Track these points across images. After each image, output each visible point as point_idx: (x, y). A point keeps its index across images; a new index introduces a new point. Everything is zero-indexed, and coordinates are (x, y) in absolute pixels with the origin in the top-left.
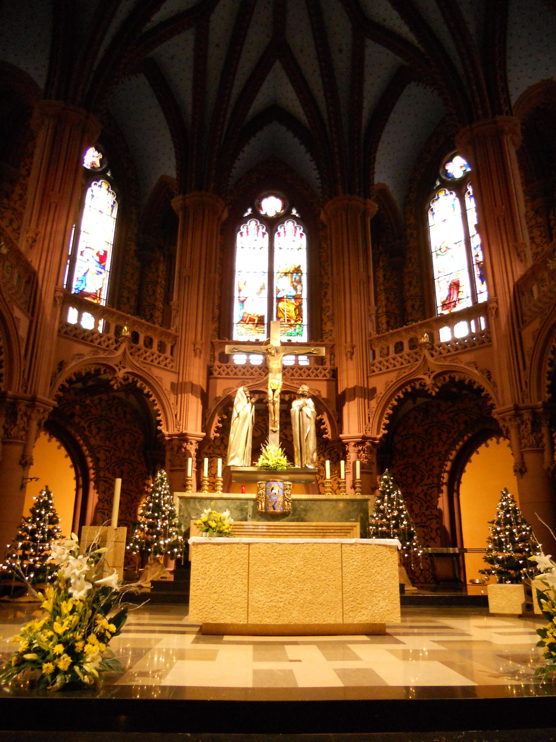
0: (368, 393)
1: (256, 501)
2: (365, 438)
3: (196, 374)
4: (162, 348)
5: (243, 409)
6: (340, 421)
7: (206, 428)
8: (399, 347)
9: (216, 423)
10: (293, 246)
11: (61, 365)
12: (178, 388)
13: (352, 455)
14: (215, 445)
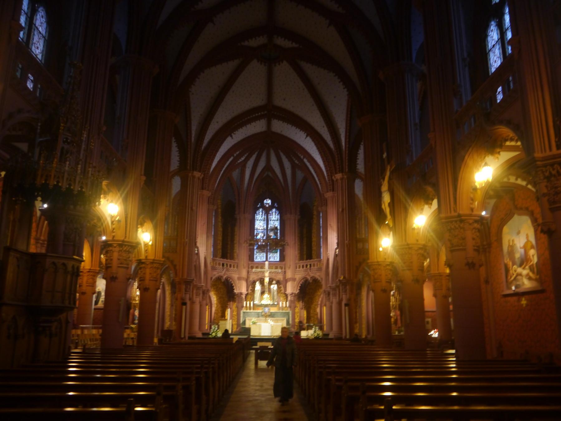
1: (262, 312)
2: (292, 293)
3: (244, 273)
4: (234, 267)
7: (247, 290)
8: (303, 267)
9: (250, 288)
11: (211, 278)
12: (240, 279)
13: (289, 298)
14: (250, 295)
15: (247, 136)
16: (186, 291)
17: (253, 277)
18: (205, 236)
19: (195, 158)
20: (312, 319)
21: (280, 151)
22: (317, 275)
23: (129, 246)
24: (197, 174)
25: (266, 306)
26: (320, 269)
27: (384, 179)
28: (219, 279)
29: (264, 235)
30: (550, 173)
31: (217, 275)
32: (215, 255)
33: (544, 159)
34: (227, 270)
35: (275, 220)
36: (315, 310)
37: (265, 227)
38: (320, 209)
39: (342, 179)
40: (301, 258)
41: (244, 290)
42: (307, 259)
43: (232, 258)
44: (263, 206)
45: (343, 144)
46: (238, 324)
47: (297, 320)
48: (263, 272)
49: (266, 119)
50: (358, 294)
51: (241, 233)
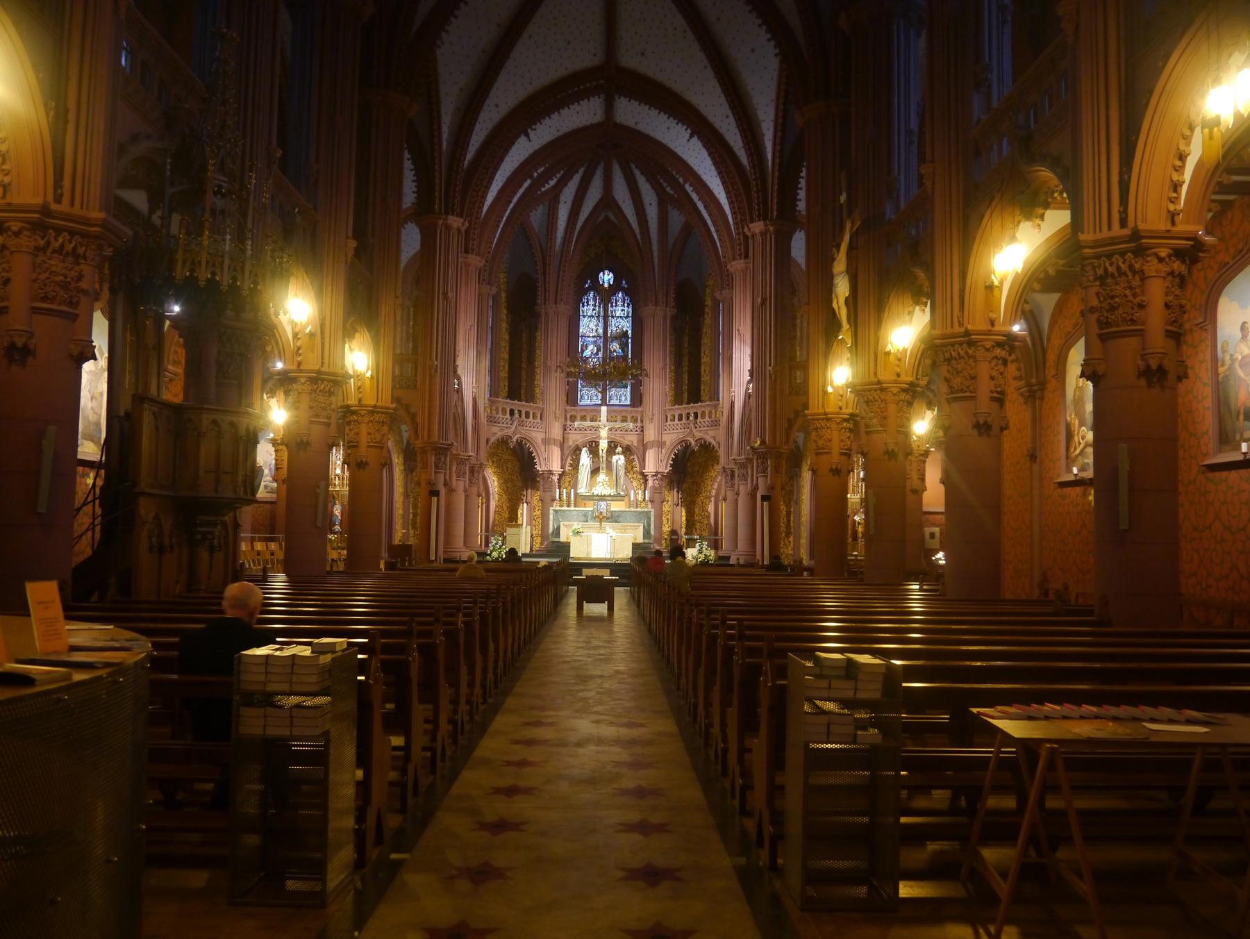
3: (556, 431)
6: (644, 460)
8: (680, 418)
9: (569, 461)
11: (488, 440)
12: (546, 442)
13: (650, 483)
15: (560, 133)
16: (437, 467)
17: (574, 438)
18: (472, 354)
19: (451, 186)
20: (698, 526)
21: (633, 166)
22: (710, 436)
23: (329, 381)
24: (455, 222)
25: (602, 498)
26: (715, 424)
27: (838, 247)
28: (504, 441)
29: (599, 350)
30: (1106, 270)
31: (499, 435)
32: (494, 392)
33: (1096, 244)
34: (521, 424)
35: (621, 320)
36: (704, 510)
37: (601, 331)
38: (717, 295)
39: (763, 234)
40: (677, 400)
41: (556, 467)
42: (688, 403)
43: (531, 398)
44: (596, 287)
45: (769, 156)
46: (544, 536)
47: (666, 529)
48: (597, 429)
49: (603, 96)
50: (794, 476)
51: (550, 348)
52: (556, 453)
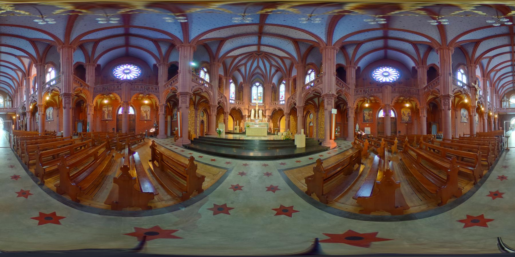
0: (270, 110)
3: (247, 107)
5: (253, 112)
10: (261, 89)
14: (249, 116)
52: (247, 111)
